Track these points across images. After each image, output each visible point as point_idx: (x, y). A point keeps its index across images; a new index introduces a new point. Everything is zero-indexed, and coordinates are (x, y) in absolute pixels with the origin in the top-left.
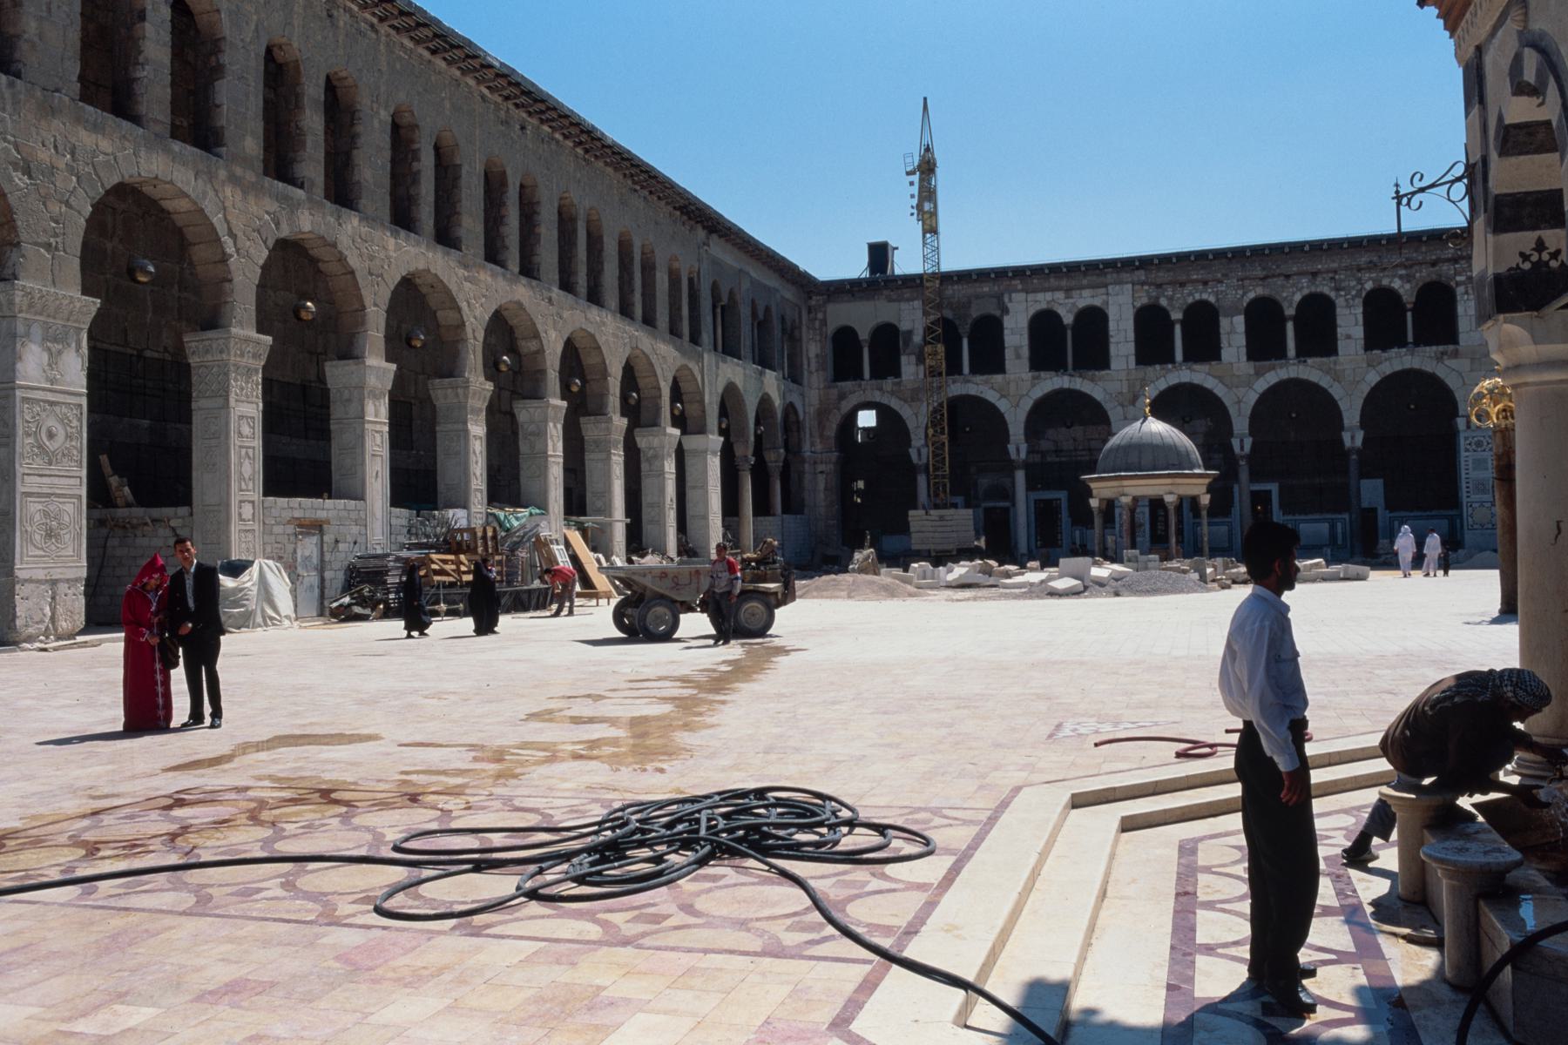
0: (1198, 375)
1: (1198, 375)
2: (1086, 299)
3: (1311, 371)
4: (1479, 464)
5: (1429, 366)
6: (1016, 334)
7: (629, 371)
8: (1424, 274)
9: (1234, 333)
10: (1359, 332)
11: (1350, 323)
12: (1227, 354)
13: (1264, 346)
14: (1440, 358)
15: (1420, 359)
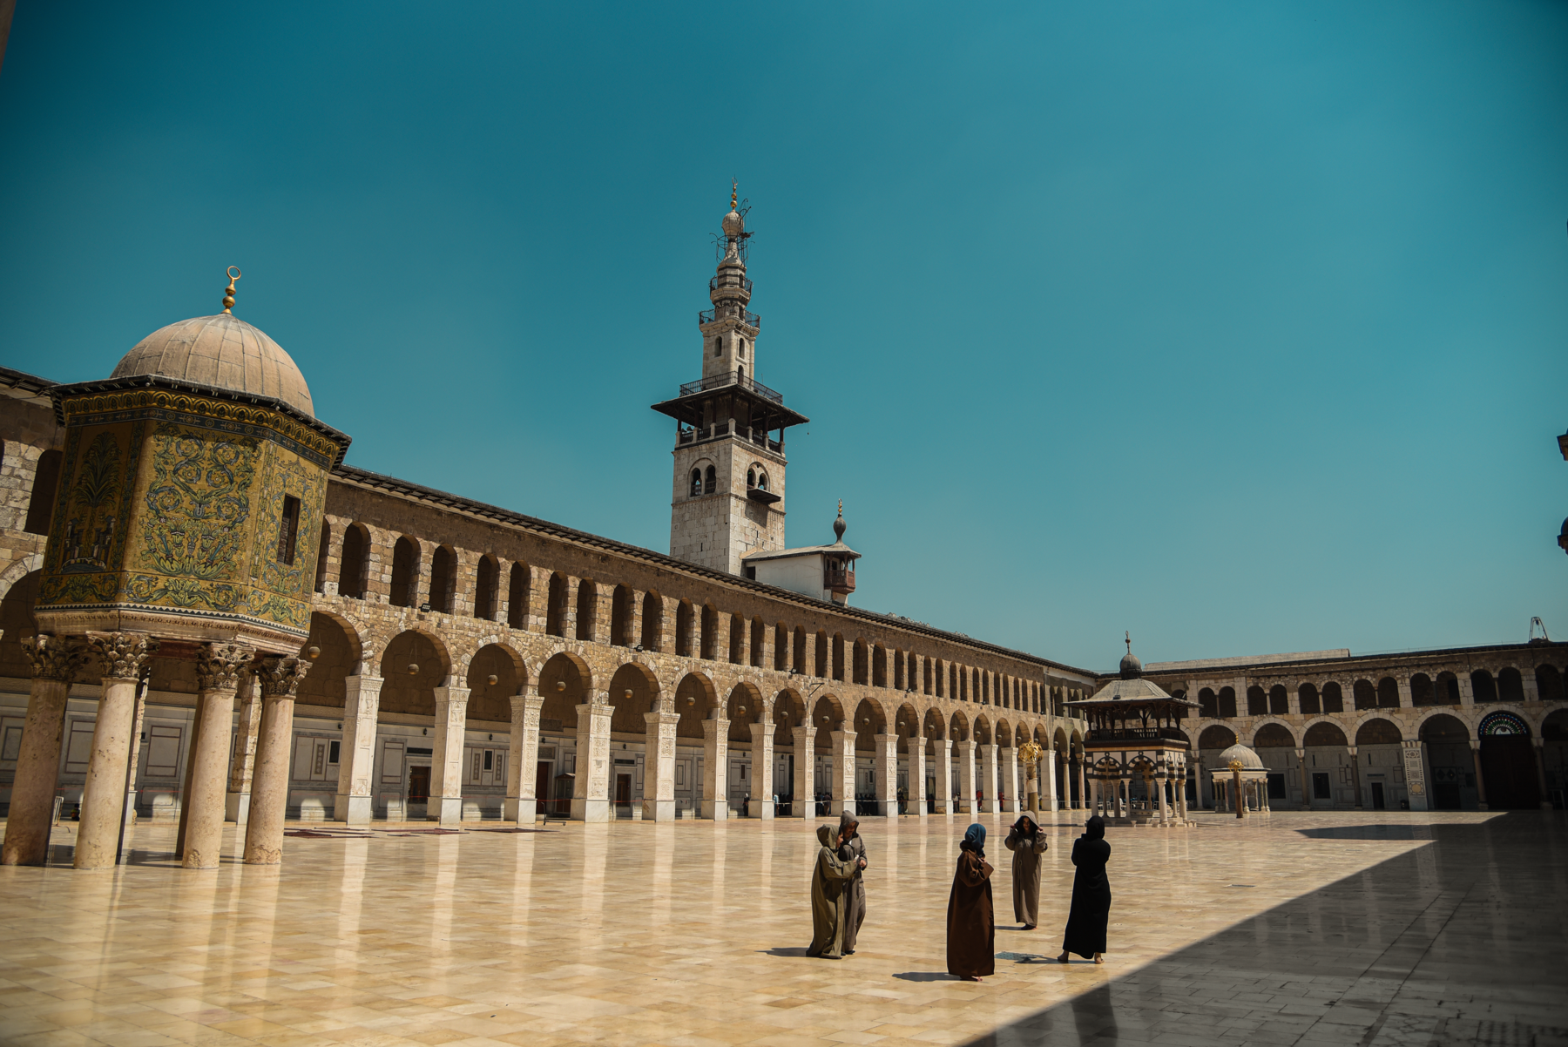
0: (1278, 719)
1: (1278, 719)
2: (1224, 683)
3: (1332, 718)
4: (1414, 764)
5: (1387, 717)
6: (1192, 697)
7: (1018, 729)
8: (1381, 674)
9: (1294, 700)
10: (1352, 701)
11: (1348, 696)
12: (1291, 710)
13: (1308, 707)
14: (1391, 713)
15: (1384, 714)
